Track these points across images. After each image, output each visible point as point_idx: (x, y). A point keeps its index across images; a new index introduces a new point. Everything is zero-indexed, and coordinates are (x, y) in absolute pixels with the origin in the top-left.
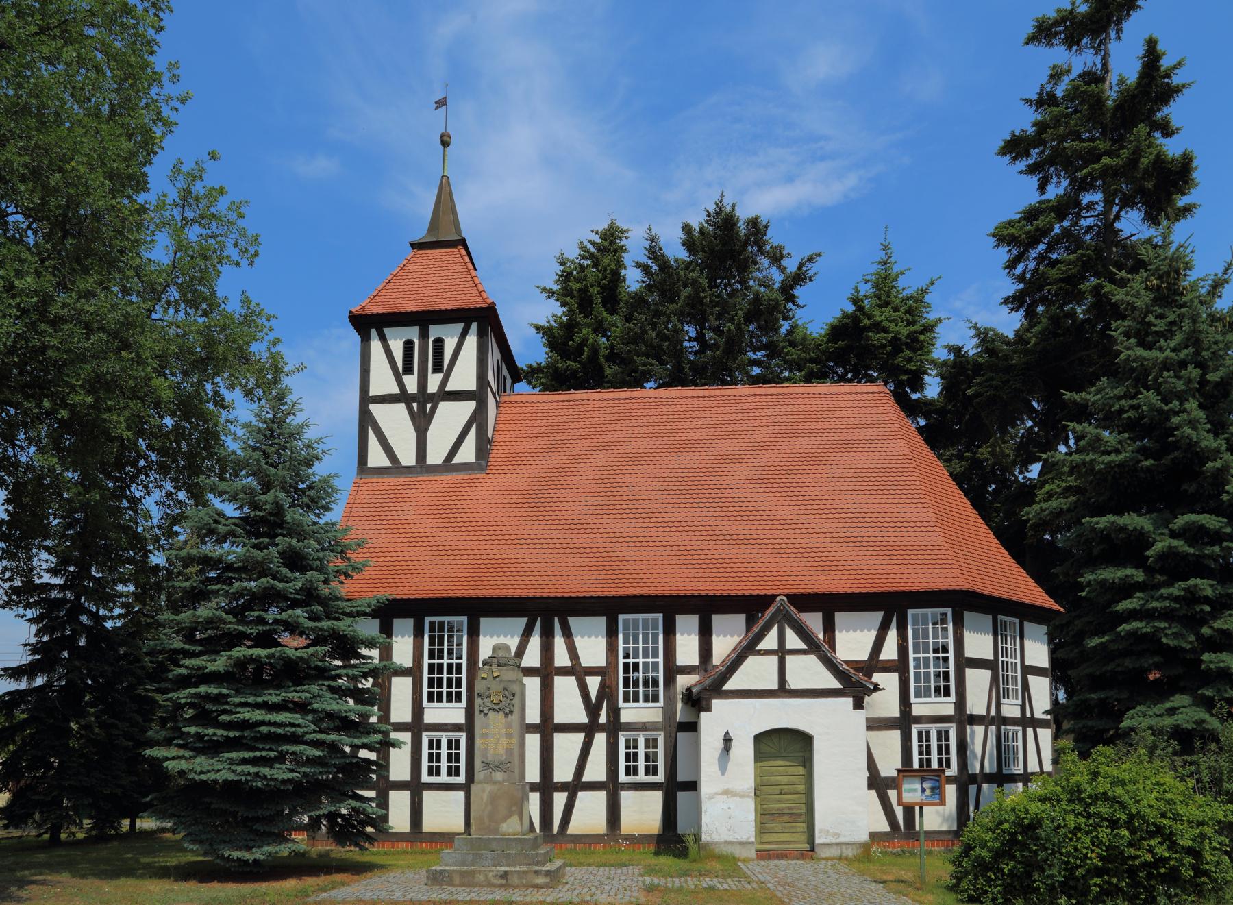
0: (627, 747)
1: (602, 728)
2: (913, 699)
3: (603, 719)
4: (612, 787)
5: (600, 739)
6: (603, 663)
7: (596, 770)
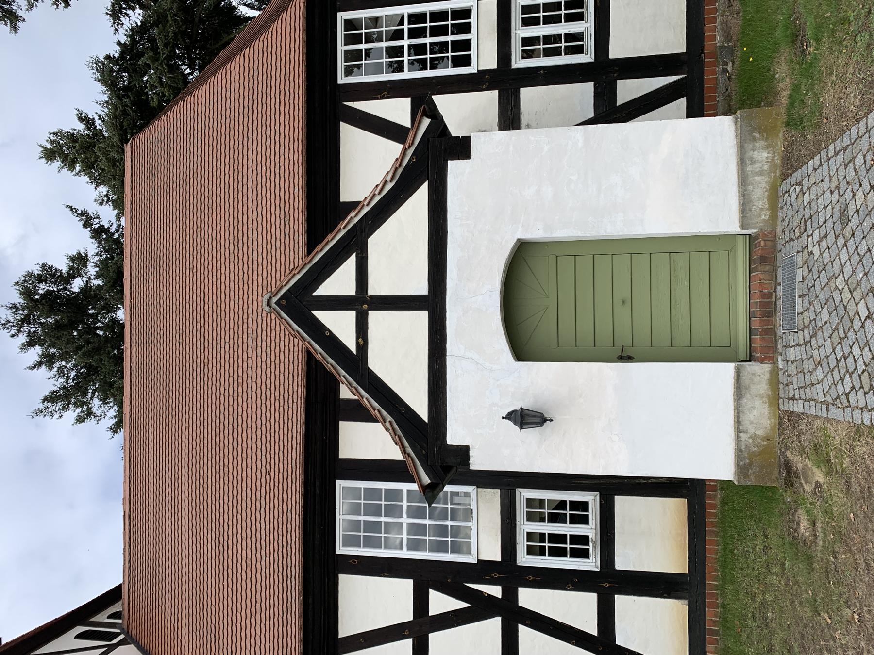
0: (541, 552)
1: (510, 595)
2: (472, 70)
3: (495, 591)
4: (609, 583)
5: (530, 598)
6: (407, 585)
7: (578, 609)
